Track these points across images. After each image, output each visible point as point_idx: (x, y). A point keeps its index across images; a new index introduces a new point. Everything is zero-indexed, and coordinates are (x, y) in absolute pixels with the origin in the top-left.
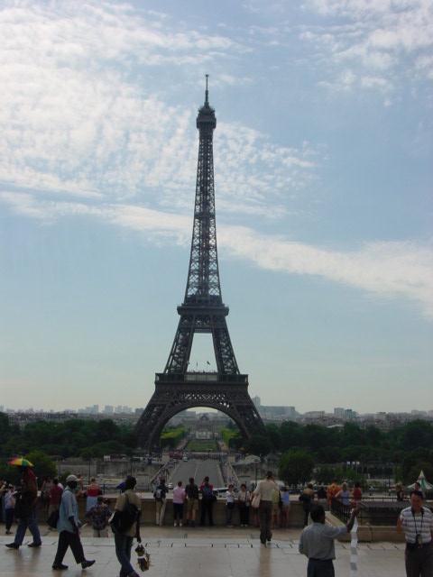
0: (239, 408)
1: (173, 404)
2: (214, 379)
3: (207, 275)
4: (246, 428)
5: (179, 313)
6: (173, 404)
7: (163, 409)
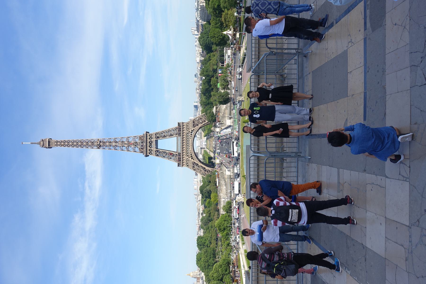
0: (194, 126)
1: (192, 159)
2: (179, 138)
3: (129, 142)
4: (204, 123)
5: (148, 156)
6: (192, 159)
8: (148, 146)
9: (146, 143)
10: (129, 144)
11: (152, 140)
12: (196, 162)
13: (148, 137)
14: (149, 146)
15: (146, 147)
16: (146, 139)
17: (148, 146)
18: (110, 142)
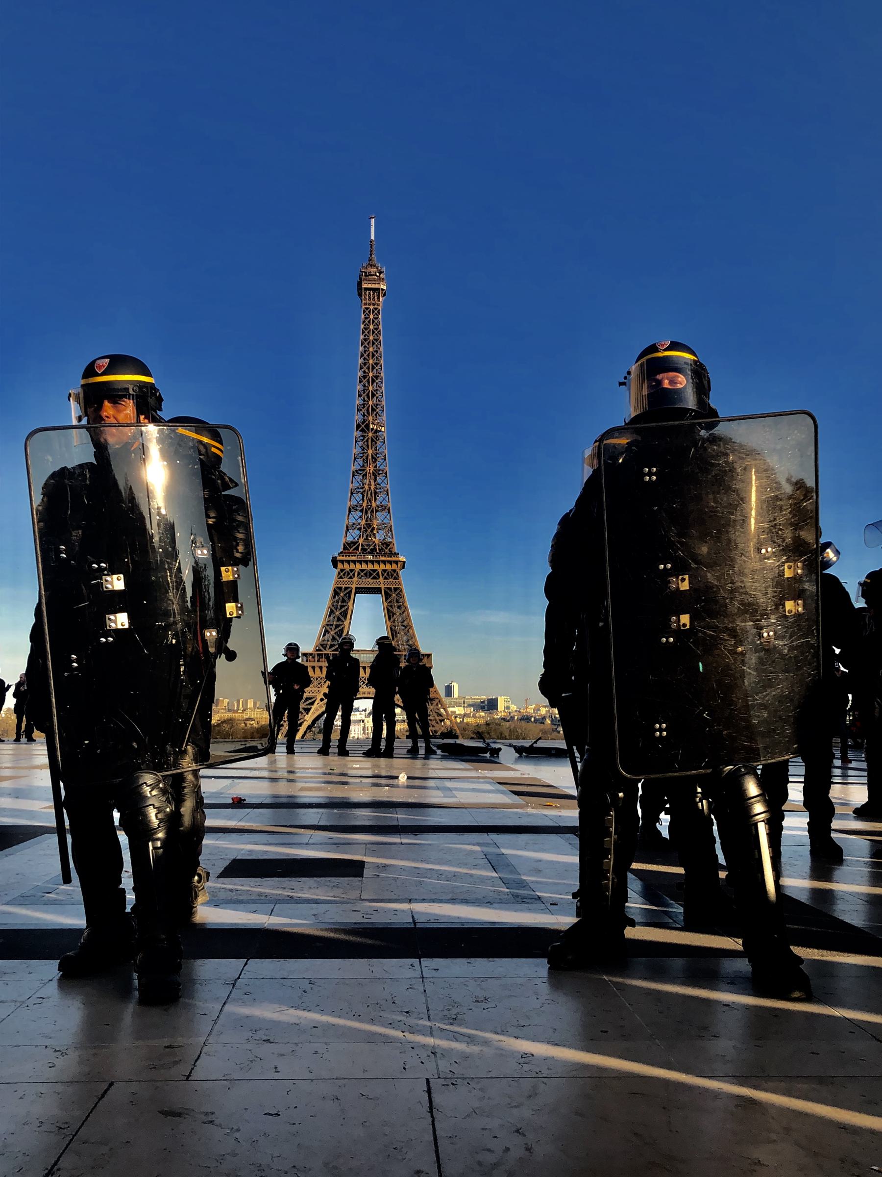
5: (335, 566)
7: (312, 703)
8: (364, 566)
9: (372, 562)
10: (369, 511)
11: (381, 579)
12: (314, 707)
13: (388, 567)
14: (362, 570)
15: (360, 562)
16: (384, 562)
17: (364, 566)
18: (374, 460)
